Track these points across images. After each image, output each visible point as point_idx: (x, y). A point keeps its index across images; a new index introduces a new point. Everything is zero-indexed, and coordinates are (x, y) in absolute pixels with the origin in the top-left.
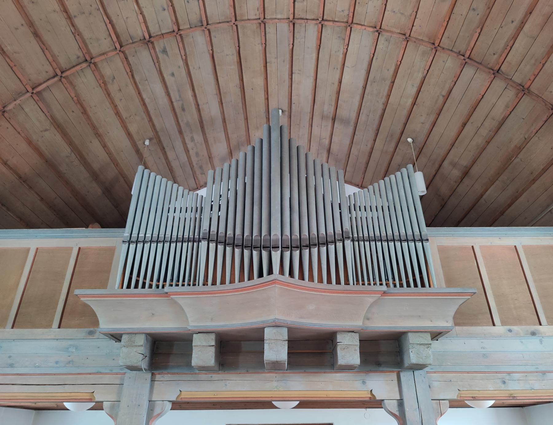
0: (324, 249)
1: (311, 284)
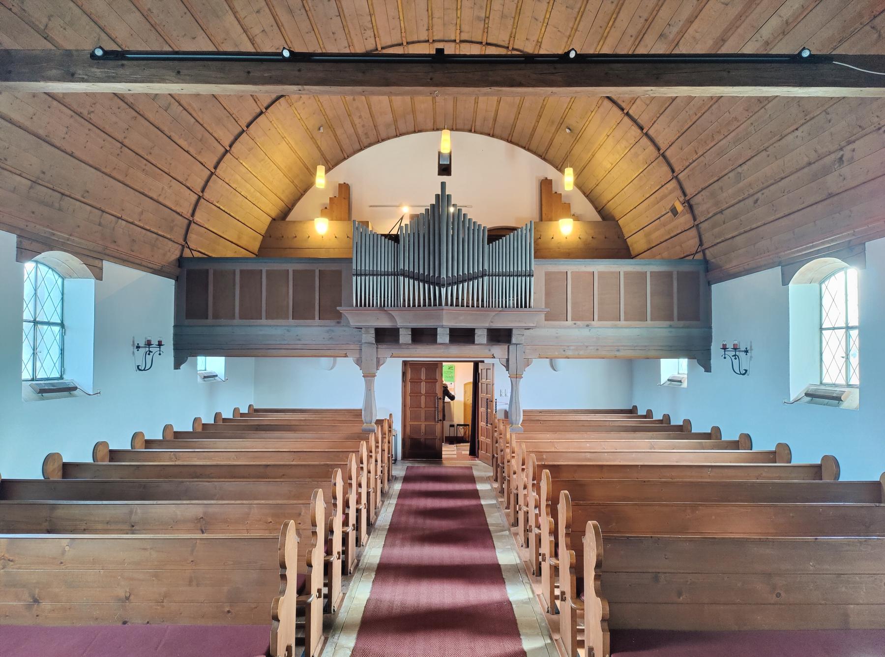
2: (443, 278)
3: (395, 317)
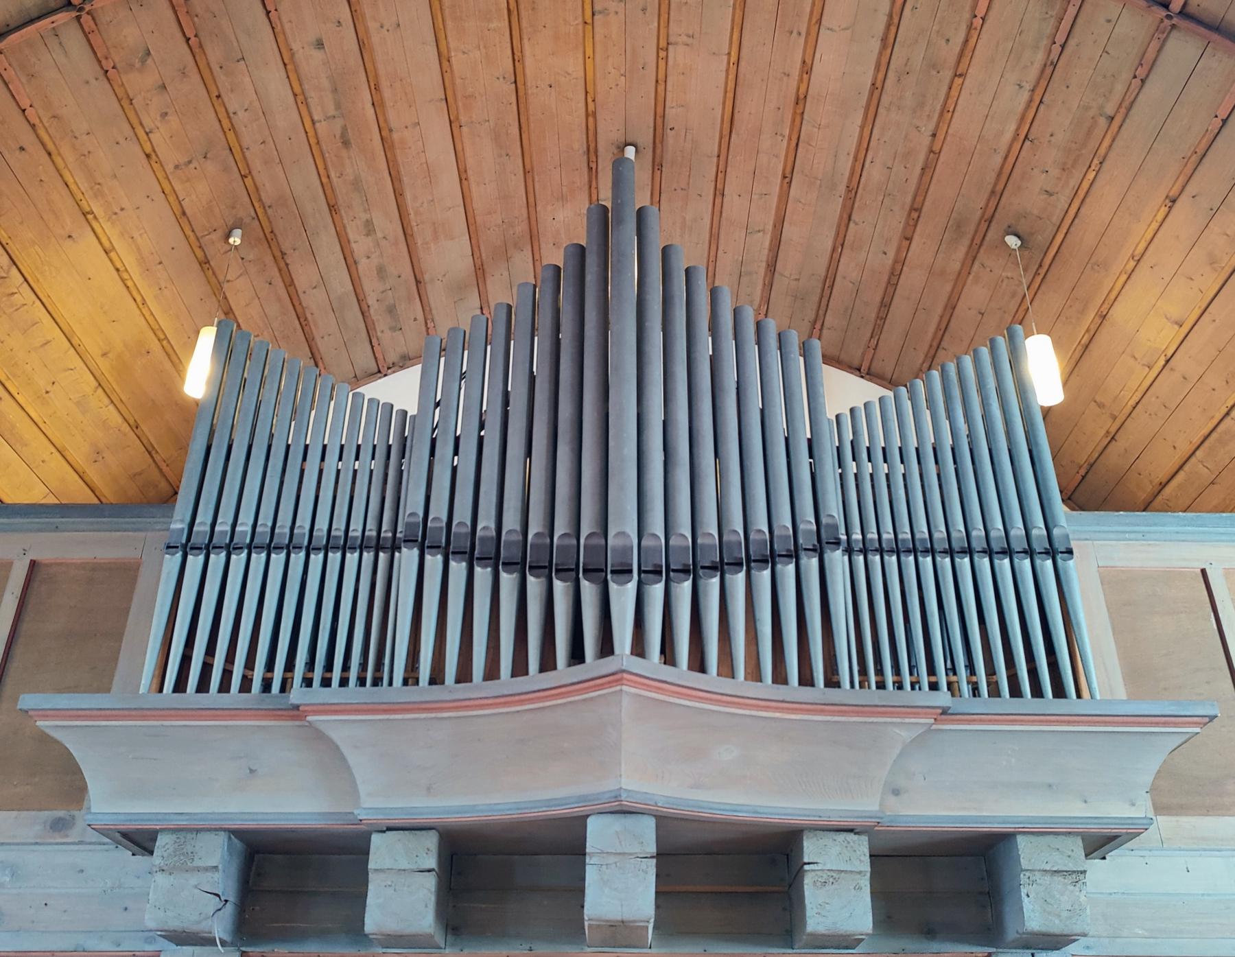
0: (764, 577)
1: (726, 685)
2: (622, 534)
3: (345, 750)
